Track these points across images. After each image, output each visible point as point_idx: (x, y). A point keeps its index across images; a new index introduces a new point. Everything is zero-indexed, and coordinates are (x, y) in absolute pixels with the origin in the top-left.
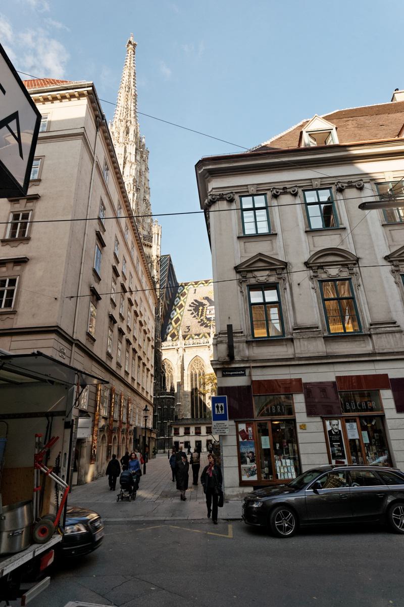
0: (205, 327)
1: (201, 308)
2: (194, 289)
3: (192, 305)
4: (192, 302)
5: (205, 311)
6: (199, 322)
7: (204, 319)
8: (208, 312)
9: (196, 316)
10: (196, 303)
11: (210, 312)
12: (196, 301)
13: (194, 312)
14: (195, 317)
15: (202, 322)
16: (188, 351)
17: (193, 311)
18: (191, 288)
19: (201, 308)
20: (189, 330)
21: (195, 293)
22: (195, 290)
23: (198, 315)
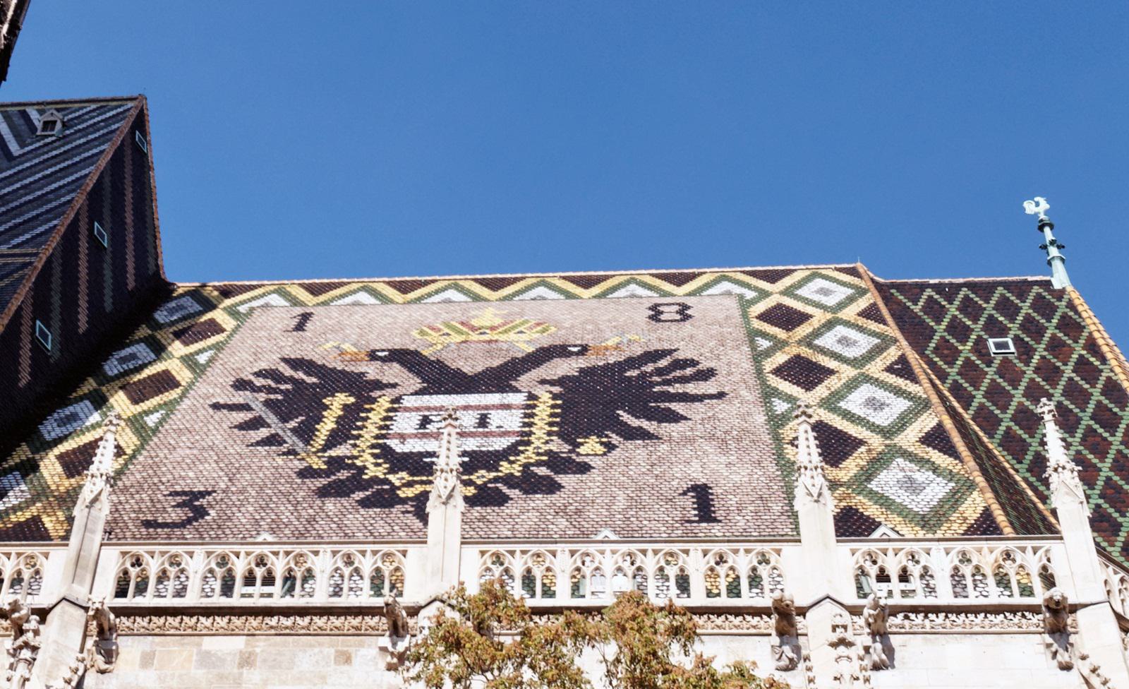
0: (365, 503)
1: (338, 402)
2: (299, 310)
3: (259, 382)
4: (263, 365)
5: (375, 417)
6: (306, 473)
7: (367, 460)
8: (406, 423)
9: (291, 440)
10: (300, 375)
11: (425, 421)
12: (295, 364)
13: (271, 418)
14: (269, 441)
15: (343, 475)
16: (147, 660)
17: (259, 410)
18: (267, 306)
19: (338, 402)
20: (201, 513)
21: (300, 327)
22: (306, 317)
23: (306, 433)
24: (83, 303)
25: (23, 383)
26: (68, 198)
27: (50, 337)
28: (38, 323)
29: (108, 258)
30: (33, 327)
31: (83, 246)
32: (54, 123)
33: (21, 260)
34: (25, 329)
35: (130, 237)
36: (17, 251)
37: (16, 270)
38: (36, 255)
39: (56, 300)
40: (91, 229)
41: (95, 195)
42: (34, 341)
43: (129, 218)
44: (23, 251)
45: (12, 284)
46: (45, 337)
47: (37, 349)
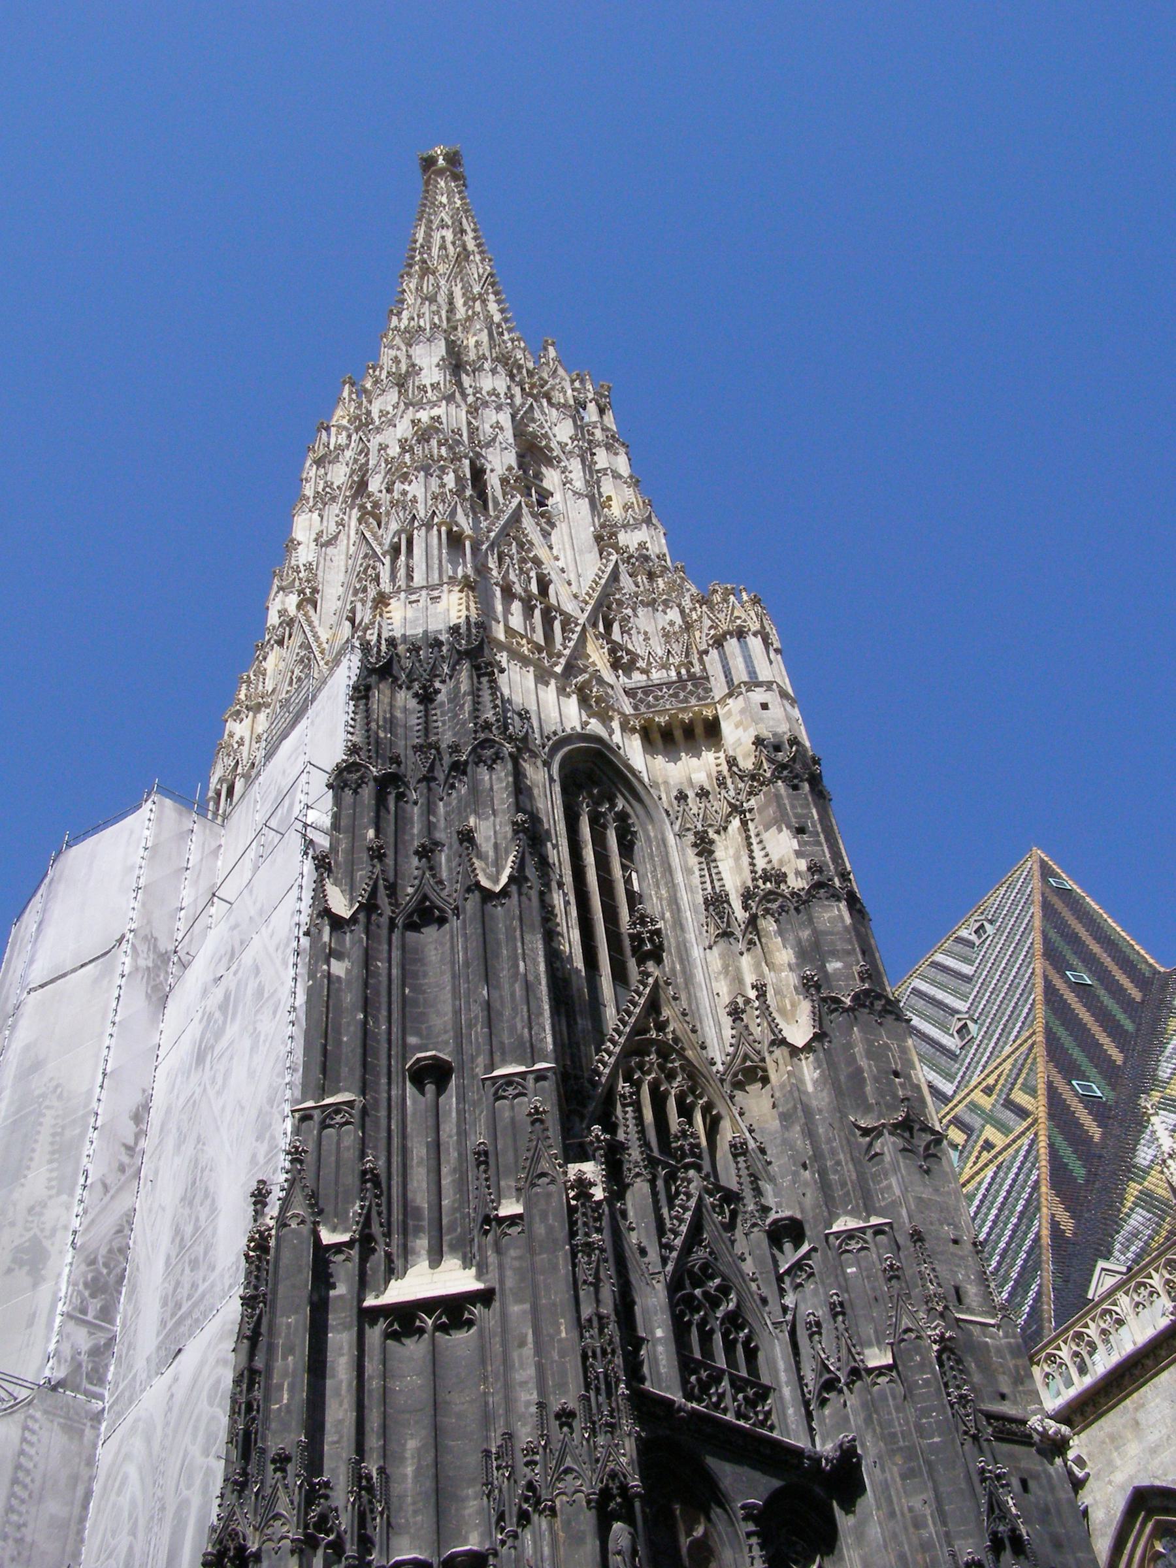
24: (1104, 1040)
25: (1097, 1138)
26: (1030, 971)
27: (1094, 1086)
28: (1074, 1082)
29: (1101, 992)
30: (1073, 1089)
31: (1071, 998)
32: (982, 926)
33: (1026, 1046)
34: (1068, 1096)
35: (1107, 961)
36: (1019, 1042)
37: (1028, 1055)
38: (1034, 1033)
39: (1077, 1054)
40: (1067, 981)
41: (1051, 954)
42: (1083, 1099)
43: (1095, 948)
44: (1023, 1038)
45: (1031, 1069)
46: (1089, 1088)
47: (1089, 1102)
